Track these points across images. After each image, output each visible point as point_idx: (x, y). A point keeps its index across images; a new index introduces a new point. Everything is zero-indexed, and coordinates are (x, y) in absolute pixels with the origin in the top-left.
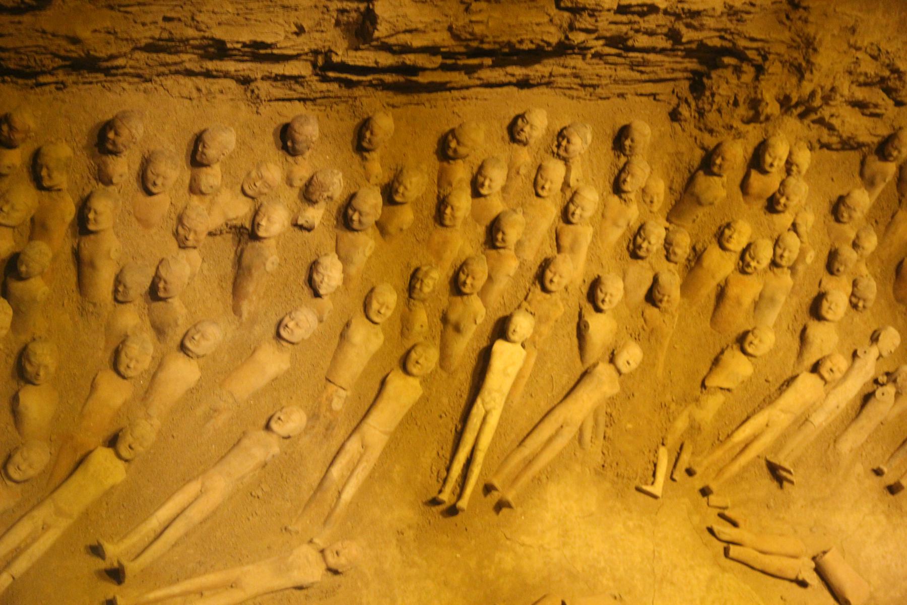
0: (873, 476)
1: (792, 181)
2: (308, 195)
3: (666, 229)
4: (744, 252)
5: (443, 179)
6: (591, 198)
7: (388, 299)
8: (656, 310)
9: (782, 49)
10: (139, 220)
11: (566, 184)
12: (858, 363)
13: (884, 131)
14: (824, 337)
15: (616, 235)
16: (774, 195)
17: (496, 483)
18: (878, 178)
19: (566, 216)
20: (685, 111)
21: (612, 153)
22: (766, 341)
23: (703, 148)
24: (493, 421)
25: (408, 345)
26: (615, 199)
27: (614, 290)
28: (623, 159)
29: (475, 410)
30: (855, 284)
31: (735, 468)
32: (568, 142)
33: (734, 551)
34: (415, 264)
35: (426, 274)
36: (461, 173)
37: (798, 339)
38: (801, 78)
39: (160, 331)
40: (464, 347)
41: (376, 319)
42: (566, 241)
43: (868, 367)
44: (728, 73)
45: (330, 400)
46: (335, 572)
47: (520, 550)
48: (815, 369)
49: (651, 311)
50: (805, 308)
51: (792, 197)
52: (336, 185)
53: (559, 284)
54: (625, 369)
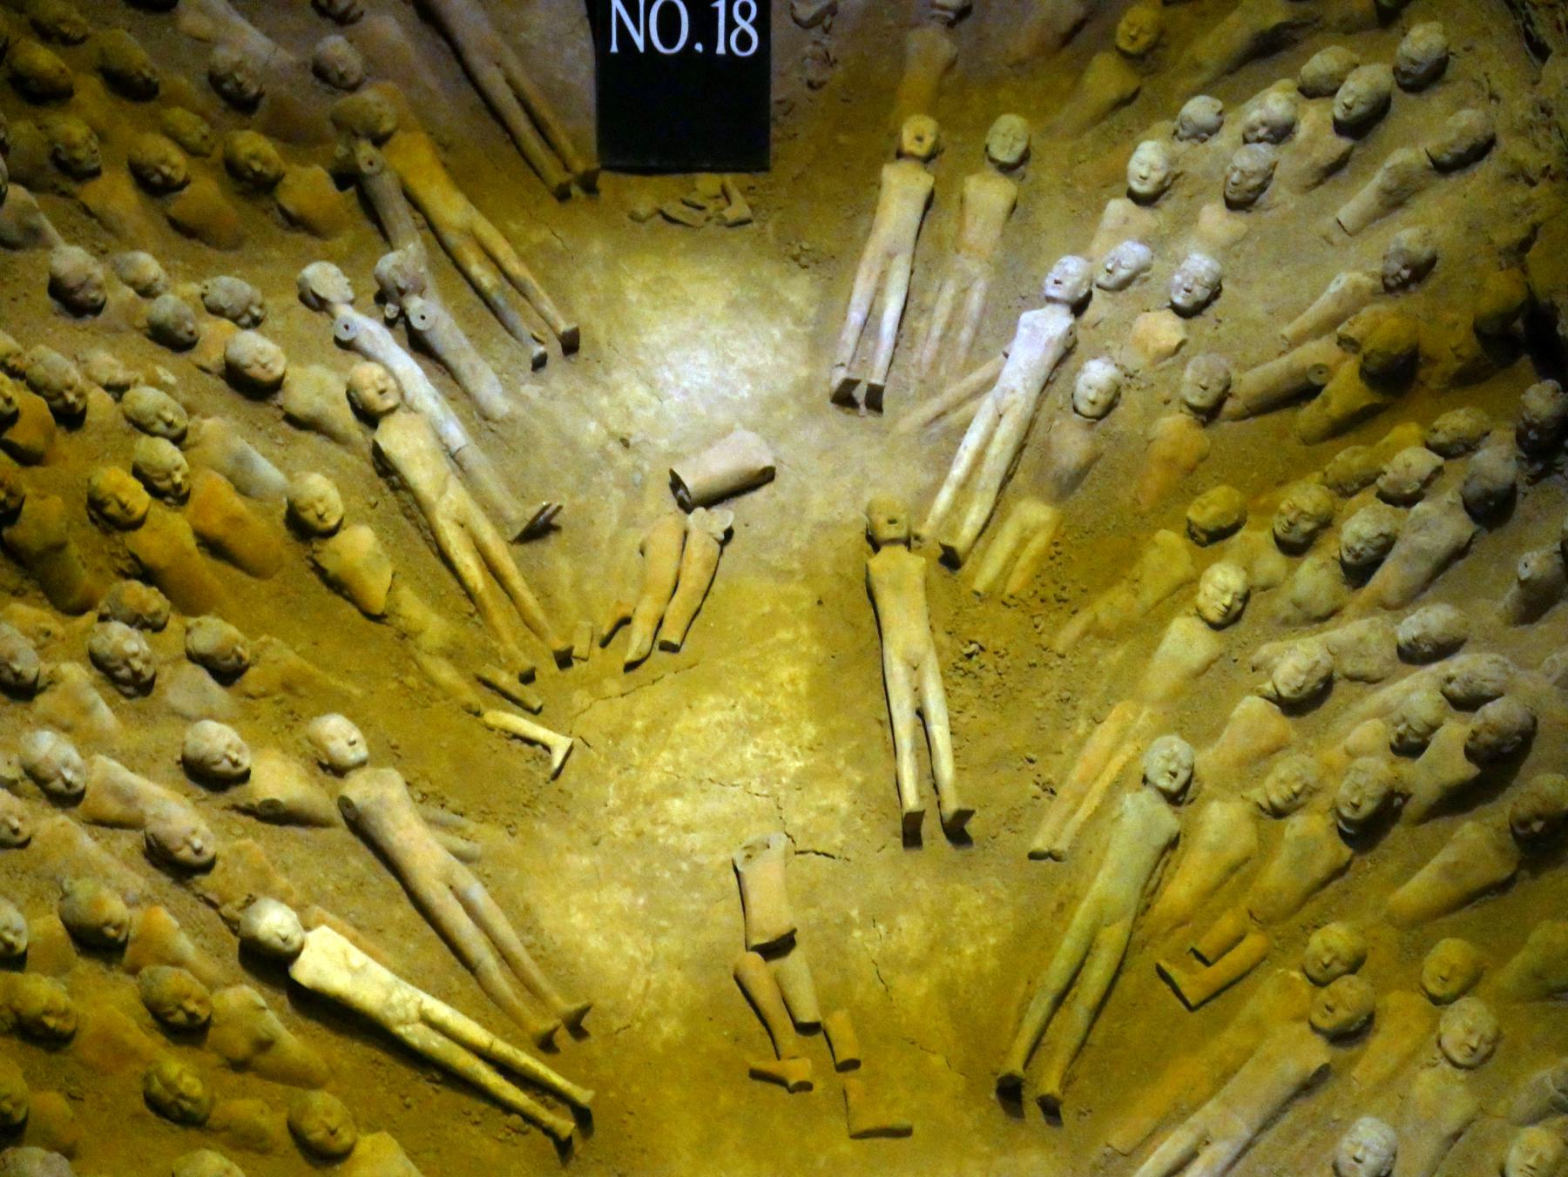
0: (544, 372)
3: (103, 618)
6: (49, 747)
8: (252, 671)
14: (315, 387)
16: (53, 410)
19: (66, 798)
22: (321, 490)
24: (441, 1011)
25: (287, 1140)
26: (43, 702)
27: (218, 739)
30: (217, 311)
31: (529, 598)
33: (671, 634)
34: (139, 1104)
35: (169, 1086)
37: (303, 435)
40: (297, 1043)
42: (113, 808)
43: (369, 329)
48: (369, 417)
49: (252, 680)
50: (245, 406)
51: (69, 380)
53: (205, 839)
54: (361, 752)
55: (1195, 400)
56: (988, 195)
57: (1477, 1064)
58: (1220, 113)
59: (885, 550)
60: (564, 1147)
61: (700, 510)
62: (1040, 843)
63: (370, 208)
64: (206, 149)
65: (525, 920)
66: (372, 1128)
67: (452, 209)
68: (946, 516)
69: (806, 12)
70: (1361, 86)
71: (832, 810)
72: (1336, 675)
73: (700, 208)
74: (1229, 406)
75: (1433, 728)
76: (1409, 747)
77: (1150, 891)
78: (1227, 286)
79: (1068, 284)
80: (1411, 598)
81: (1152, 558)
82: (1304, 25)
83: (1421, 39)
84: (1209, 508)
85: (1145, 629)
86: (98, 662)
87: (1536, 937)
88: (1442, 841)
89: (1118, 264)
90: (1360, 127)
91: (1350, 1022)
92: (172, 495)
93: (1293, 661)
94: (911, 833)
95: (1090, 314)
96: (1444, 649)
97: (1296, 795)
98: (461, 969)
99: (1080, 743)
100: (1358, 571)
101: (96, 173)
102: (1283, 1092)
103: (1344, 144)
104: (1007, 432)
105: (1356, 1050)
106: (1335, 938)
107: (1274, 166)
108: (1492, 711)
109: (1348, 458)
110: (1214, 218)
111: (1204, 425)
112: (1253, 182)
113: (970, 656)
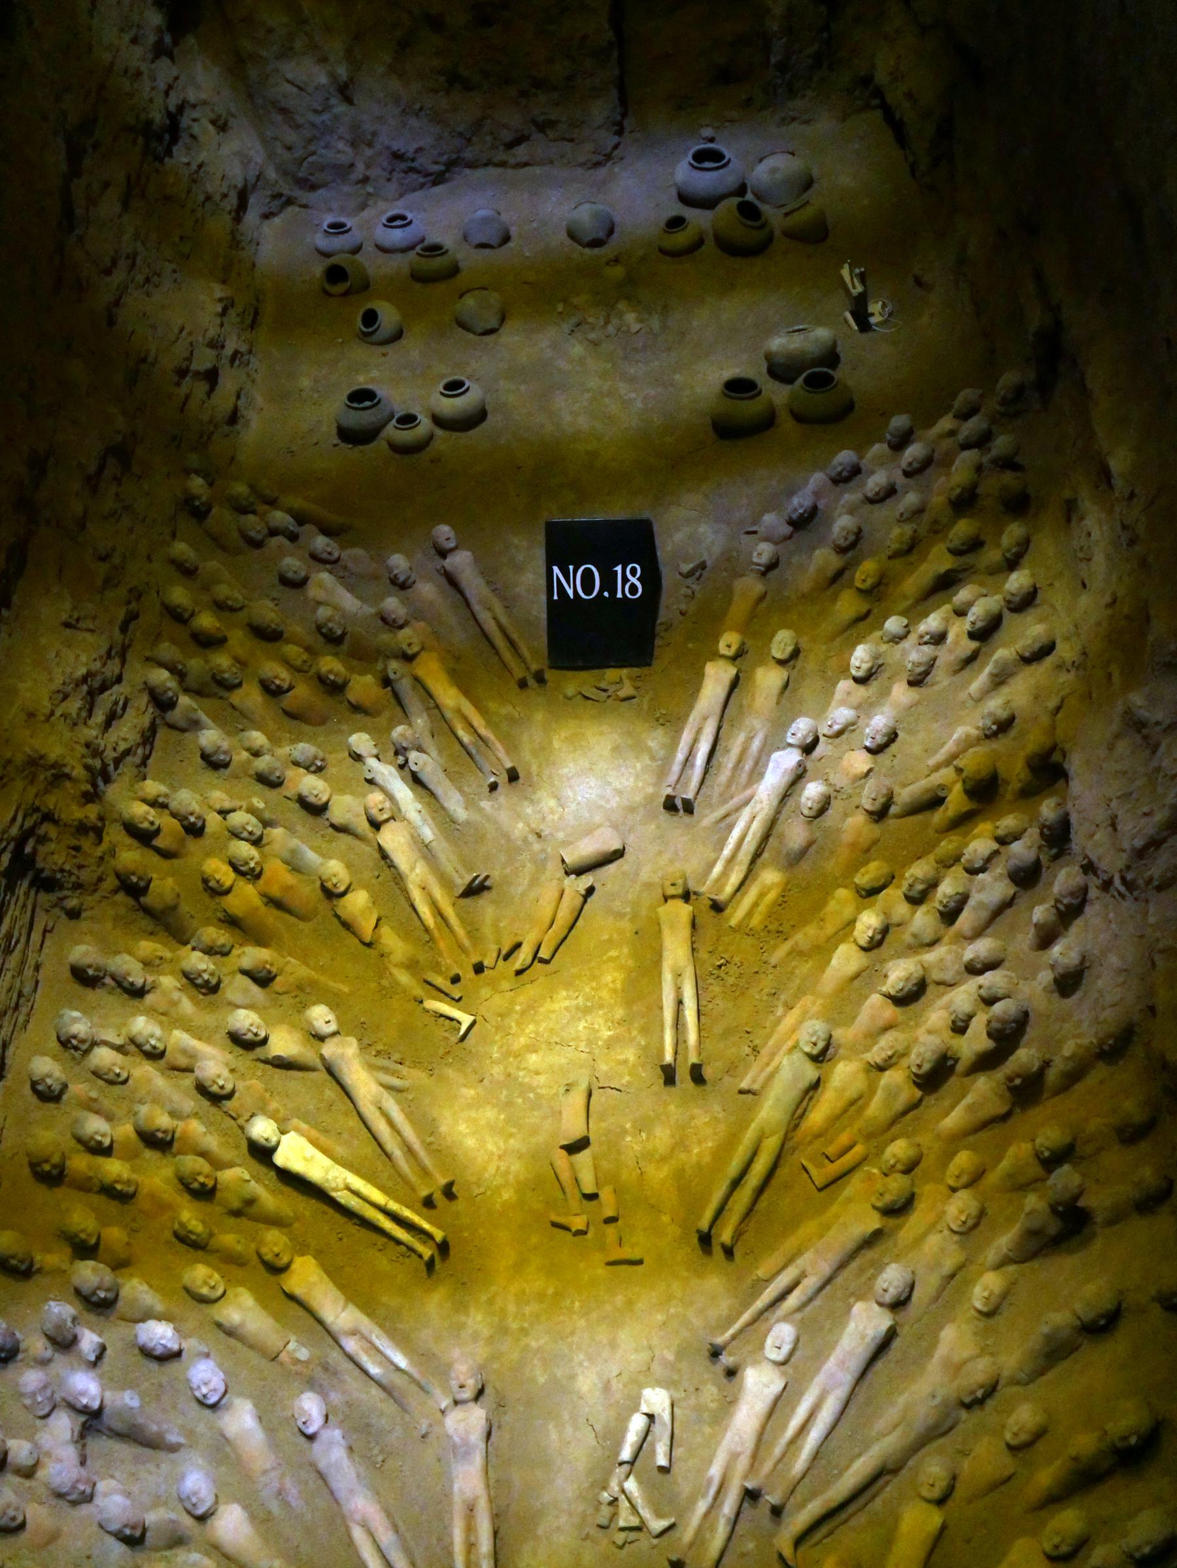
0: (495, 794)
1: (174, 805)
2: (64, 1343)
3: (194, 949)
4: (235, 869)
6: (142, 1025)
7: (201, 1275)
8: (278, 978)
9: (32, 791)
10: (48, 1543)
11: (119, 1049)
12: (379, 780)
13: (145, 698)
14: (346, 807)
16: (184, 827)
17: (424, 1193)
18: (193, 716)
19: (155, 1055)
20: (72, 903)
21: (98, 991)
22: (335, 870)
23: (115, 892)
25: (255, 1259)
26: (149, 999)
27: (245, 1020)
28: (108, 980)
29: (342, 1201)
30: (296, 764)
31: (460, 932)
32: (75, 1037)
33: (544, 954)
34: (168, 1235)
35: (182, 1225)
36: (80, 1163)
37: (341, 835)
38: (68, 777)
41: (220, 1292)
42: (182, 1061)
43: (386, 773)
44: (43, 850)
45: (297, 1361)
46: (480, 1393)
47: (499, 1181)
48: (376, 825)
49: (278, 984)
50: (311, 819)
51: (191, 809)
52: (61, 1310)
53: (225, 1080)
54: (333, 1027)
55: (869, 807)
58: (906, 626)
59: (669, 901)
61: (573, 876)
62: (744, 1085)
64: (305, 668)
65: (427, 1126)
67: (449, 696)
68: (718, 880)
70: (978, 612)
71: (625, 1061)
72: (928, 981)
73: (605, 691)
74: (894, 810)
75: (970, 1017)
76: (960, 1027)
78: (901, 734)
79: (799, 735)
80: (978, 933)
81: (832, 906)
82: (965, 570)
85: (822, 951)
89: (835, 722)
90: (985, 633)
91: (894, 1202)
93: (899, 972)
94: (669, 1076)
95: (819, 751)
97: (890, 1057)
98: (384, 1157)
99: (778, 1021)
101: (239, 685)
102: (850, 1246)
103: (974, 645)
104: (757, 828)
105: (900, 1220)
107: (935, 659)
108: (998, 1008)
109: (947, 846)
110: (901, 693)
111: (877, 821)
112: (921, 669)
113: (720, 966)
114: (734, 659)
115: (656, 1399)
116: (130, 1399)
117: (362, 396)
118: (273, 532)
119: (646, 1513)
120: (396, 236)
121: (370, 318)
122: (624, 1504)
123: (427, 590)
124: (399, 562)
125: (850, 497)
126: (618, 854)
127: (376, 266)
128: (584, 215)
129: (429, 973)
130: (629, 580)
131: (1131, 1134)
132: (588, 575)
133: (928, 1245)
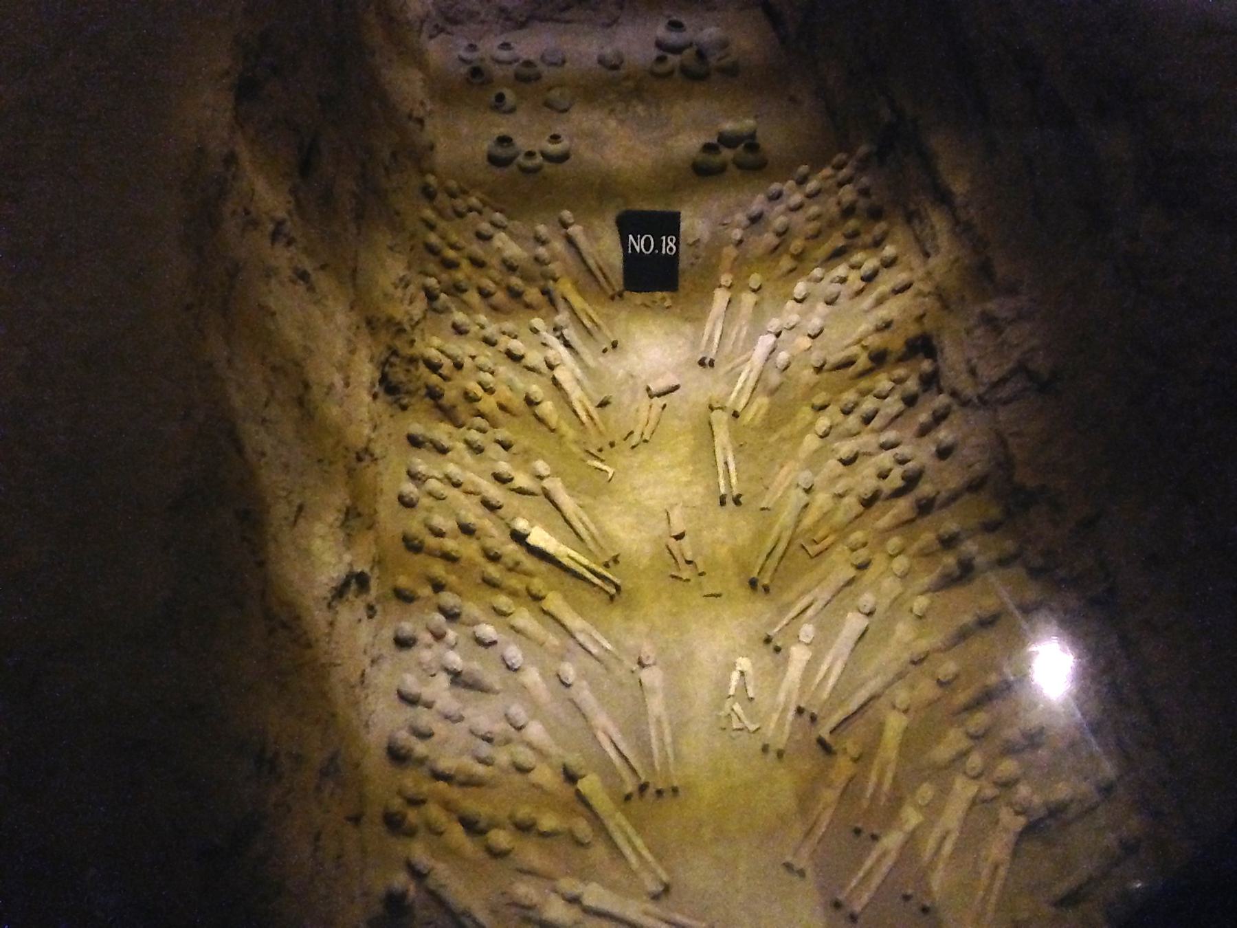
2: (439, 636)
5: (431, 553)
6: (452, 469)
7: (503, 601)
13: (423, 294)
14: (534, 358)
15: (468, 458)
19: (457, 485)
20: (405, 401)
22: (536, 389)
24: (573, 554)
25: (525, 593)
26: (450, 454)
27: (504, 467)
30: (504, 333)
33: (646, 437)
34: (479, 581)
36: (431, 541)
38: (404, 331)
39: (508, 741)
40: (529, 563)
42: (471, 488)
43: (552, 339)
45: (555, 646)
48: (551, 367)
49: (514, 449)
56: (748, 299)
57: (904, 576)
60: (612, 598)
63: (552, 302)
65: (600, 529)
66: (551, 589)
67: (577, 301)
69: (691, 240)
75: (890, 470)
77: (798, 522)
80: (882, 429)
81: (800, 416)
83: (889, 250)
84: (819, 400)
86: (467, 442)
87: (923, 537)
88: (892, 507)
90: (869, 279)
92: (489, 391)
93: (846, 448)
96: (894, 445)
99: (777, 473)
100: (867, 420)
101: (465, 291)
103: (863, 284)
106: (858, 536)
108: (910, 465)
109: (864, 384)
110: (821, 308)
114: (729, 288)
115: (744, 663)
116: (475, 665)
117: (504, 140)
118: (471, 209)
119: (747, 722)
120: (504, 55)
121: (500, 98)
122: (735, 719)
123: (559, 245)
124: (542, 229)
125: (780, 208)
126: (677, 388)
127: (498, 71)
128: (608, 51)
129: (598, 443)
130: (668, 245)
131: (989, 527)
132: (647, 240)
133: (882, 586)
